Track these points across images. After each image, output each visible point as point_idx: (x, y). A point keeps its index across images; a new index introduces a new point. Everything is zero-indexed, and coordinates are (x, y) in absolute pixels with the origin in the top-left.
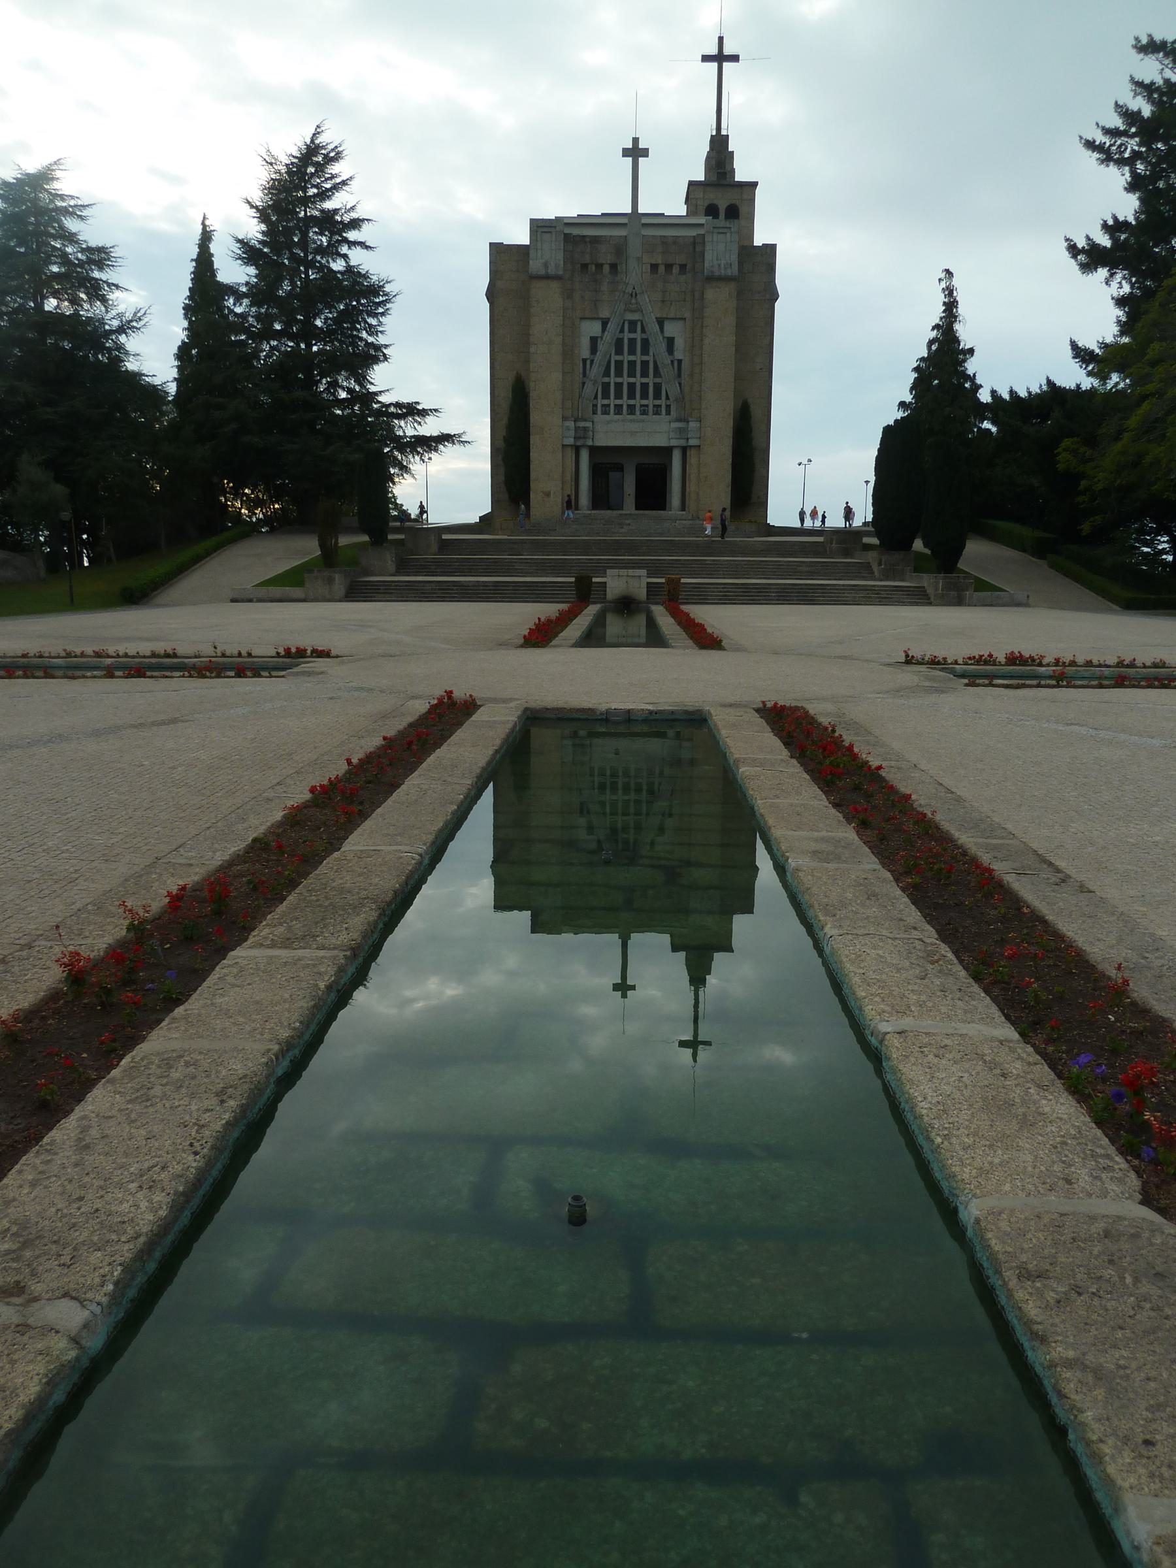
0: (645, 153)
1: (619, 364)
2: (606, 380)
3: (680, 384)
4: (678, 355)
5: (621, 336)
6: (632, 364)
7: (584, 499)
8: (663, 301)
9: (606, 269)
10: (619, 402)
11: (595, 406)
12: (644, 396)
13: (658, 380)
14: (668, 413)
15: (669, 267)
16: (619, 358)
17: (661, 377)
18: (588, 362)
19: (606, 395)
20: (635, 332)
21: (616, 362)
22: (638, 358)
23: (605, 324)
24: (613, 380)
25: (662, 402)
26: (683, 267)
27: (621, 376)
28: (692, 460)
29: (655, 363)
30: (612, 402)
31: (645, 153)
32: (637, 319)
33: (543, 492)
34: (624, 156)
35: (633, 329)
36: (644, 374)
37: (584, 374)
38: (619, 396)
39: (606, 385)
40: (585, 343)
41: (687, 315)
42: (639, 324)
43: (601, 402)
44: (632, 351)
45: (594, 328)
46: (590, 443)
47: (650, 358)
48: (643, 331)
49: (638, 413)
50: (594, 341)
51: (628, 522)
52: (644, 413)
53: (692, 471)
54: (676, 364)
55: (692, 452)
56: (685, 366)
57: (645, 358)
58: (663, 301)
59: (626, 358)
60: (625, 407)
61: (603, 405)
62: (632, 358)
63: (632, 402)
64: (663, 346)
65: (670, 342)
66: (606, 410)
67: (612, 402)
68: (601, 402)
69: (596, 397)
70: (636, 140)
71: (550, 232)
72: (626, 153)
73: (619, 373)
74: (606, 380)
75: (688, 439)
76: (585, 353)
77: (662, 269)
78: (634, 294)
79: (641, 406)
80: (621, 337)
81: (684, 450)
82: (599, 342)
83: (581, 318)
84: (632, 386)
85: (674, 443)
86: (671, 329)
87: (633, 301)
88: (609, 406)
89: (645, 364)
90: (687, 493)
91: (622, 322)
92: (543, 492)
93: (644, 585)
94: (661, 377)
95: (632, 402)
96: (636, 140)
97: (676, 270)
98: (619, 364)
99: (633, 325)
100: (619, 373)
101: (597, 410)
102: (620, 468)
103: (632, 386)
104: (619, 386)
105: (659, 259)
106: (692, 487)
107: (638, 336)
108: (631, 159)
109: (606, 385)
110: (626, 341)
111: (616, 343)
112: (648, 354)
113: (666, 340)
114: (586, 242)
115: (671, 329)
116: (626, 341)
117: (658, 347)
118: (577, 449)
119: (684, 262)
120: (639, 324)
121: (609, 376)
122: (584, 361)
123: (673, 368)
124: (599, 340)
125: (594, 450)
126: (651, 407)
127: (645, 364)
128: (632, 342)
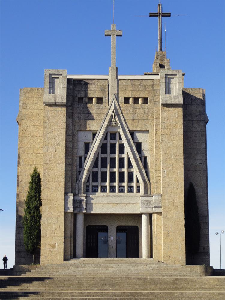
2: (95, 170)
5: (105, 142)
8: (133, 120)
9: (94, 100)
11: (88, 187)
14: (138, 191)
15: (136, 100)
16: (104, 156)
18: (83, 158)
21: (102, 158)
24: (99, 170)
29: (129, 159)
33: (50, 245)
40: (81, 146)
43: (91, 184)
51: (111, 265)
52: (121, 190)
58: (133, 120)
59: (109, 156)
61: (93, 186)
68: (91, 184)
69: (88, 181)
73: (104, 166)
74: (95, 170)
76: (82, 153)
77: (131, 100)
80: (106, 142)
81: (150, 216)
92: (50, 245)
97: (140, 101)
101: (89, 190)
102: (105, 229)
110: (109, 145)
112: (124, 153)
113: (136, 144)
114: (81, 84)
116: (109, 145)
119: (146, 96)
121: (97, 167)
125: (88, 216)
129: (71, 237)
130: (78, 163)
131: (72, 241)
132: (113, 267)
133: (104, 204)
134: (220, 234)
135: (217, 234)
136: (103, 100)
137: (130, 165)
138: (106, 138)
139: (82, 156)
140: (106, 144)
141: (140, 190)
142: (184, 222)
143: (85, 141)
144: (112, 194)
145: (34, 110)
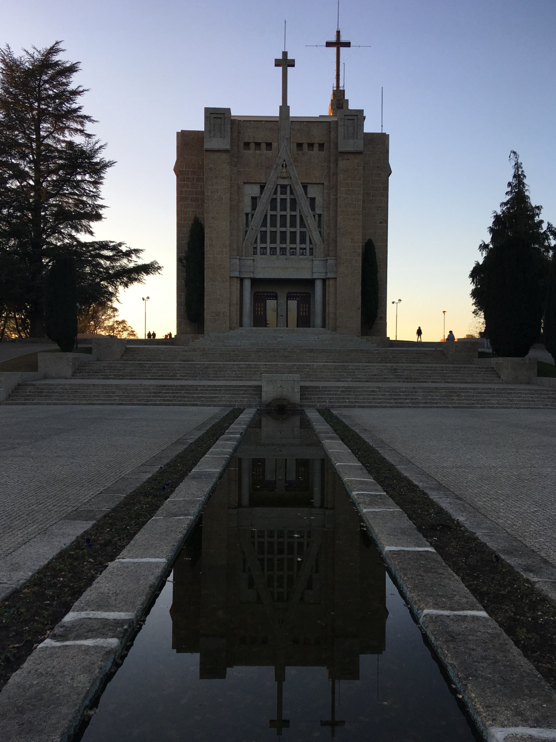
0: (292, 64)
1: (273, 217)
2: (263, 229)
3: (320, 232)
4: (318, 211)
5: (274, 197)
7: (247, 319)
10: (273, 245)
11: (255, 248)
12: (293, 241)
13: (303, 230)
14: (311, 254)
15: (311, 145)
16: (273, 213)
17: (305, 227)
18: (250, 216)
19: (264, 241)
20: (286, 194)
22: (288, 213)
23: (262, 188)
24: (269, 229)
25: (307, 246)
26: (321, 146)
27: (276, 226)
28: (331, 289)
29: (301, 216)
30: (269, 245)
31: (292, 64)
32: (287, 184)
34: (276, 65)
35: (284, 192)
36: (293, 225)
37: (247, 225)
38: (273, 241)
39: (264, 234)
40: (248, 202)
42: (288, 188)
43: (259, 245)
44: (284, 209)
45: (254, 190)
47: (297, 213)
48: (292, 193)
49: (288, 254)
50: (254, 200)
52: (293, 254)
53: (330, 298)
54: (317, 216)
55: (330, 282)
56: (325, 218)
57: (293, 213)
59: (279, 213)
60: (278, 250)
61: (261, 248)
62: (283, 213)
63: (284, 246)
64: (308, 203)
65: (313, 200)
66: (263, 251)
67: (269, 245)
68: (259, 245)
69: (256, 242)
70: (285, 54)
71: (221, 118)
72: (278, 63)
73: (273, 225)
74: (263, 229)
76: (248, 210)
78: (284, 165)
79: (291, 249)
80: (275, 197)
81: (324, 281)
82: (258, 200)
83: (244, 183)
84: (283, 234)
85: (315, 276)
86: (313, 192)
87: (284, 170)
88: (266, 248)
89: (293, 217)
90: (327, 315)
93: (297, 389)
94: (305, 227)
95: (284, 246)
96: (285, 54)
98: (273, 217)
99: (284, 187)
100: (273, 225)
101: (256, 252)
103: (283, 234)
104: (273, 233)
105: (304, 140)
106: (330, 309)
107: (288, 197)
108: (281, 68)
109: (264, 234)
110: (279, 200)
111: (270, 202)
113: (309, 199)
115: (313, 192)
116: (279, 200)
117: (304, 205)
118: (242, 280)
120: (288, 188)
121: (266, 226)
122: (247, 214)
123: (315, 219)
124: (258, 198)
125: (255, 282)
126: (298, 249)
127: (293, 217)
128: (283, 201)
129: (237, 304)
130: (245, 221)
131: (239, 309)
132: (282, 337)
137: (303, 224)
138: (275, 193)
139: (249, 213)
140: (276, 199)
141: (312, 252)
142: (360, 289)
143: (252, 196)
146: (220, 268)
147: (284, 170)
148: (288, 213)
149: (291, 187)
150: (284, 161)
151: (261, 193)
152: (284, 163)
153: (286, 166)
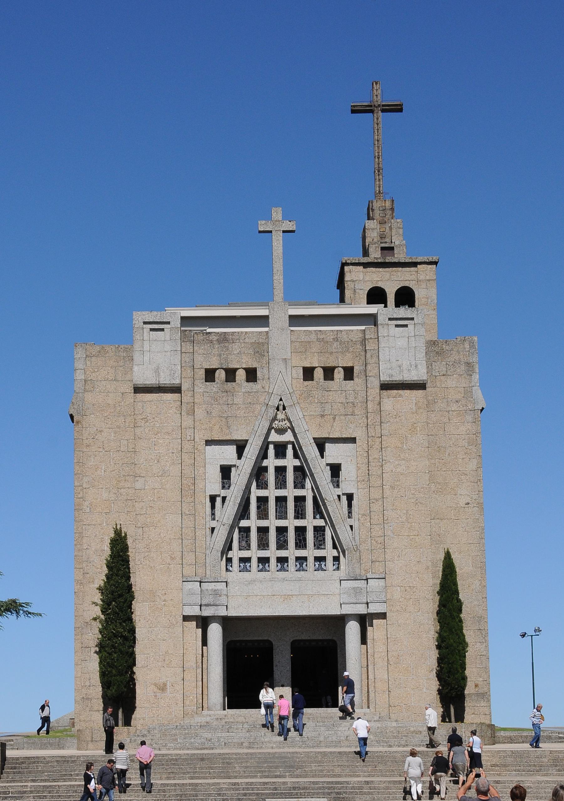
6: (281, 501)
18: (219, 500)
22: (290, 492)
23: (241, 447)
29: (315, 498)
33: (155, 685)
36: (300, 514)
41: (359, 434)
42: (290, 447)
46: (222, 612)
48: (296, 456)
54: (344, 498)
65: (335, 470)
75: (367, 603)
78: (281, 408)
91: (266, 444)
92: (155, 685)
97: (339, 374)
119: (350, 364)
120: (290, 447)
122: (213, 499)
133: (264, 596)
134: (532, 636)
135: (523, 635)
136: (259, 374)
144: (282, 574)
145: (110, 395)
146: (165, 601)
147: (280, 416)
148: (290, 492)
149: (293, 443)
150: (281, 400)
151: (240, 456)
152: (281, 402)
153: (284, 408)
